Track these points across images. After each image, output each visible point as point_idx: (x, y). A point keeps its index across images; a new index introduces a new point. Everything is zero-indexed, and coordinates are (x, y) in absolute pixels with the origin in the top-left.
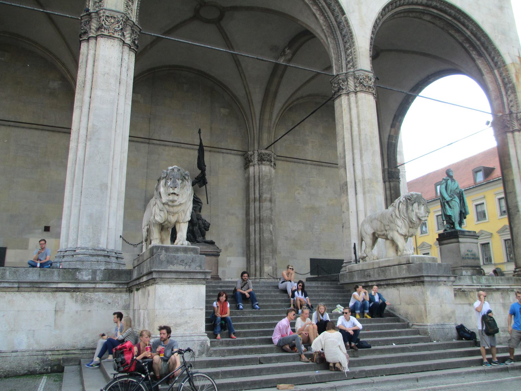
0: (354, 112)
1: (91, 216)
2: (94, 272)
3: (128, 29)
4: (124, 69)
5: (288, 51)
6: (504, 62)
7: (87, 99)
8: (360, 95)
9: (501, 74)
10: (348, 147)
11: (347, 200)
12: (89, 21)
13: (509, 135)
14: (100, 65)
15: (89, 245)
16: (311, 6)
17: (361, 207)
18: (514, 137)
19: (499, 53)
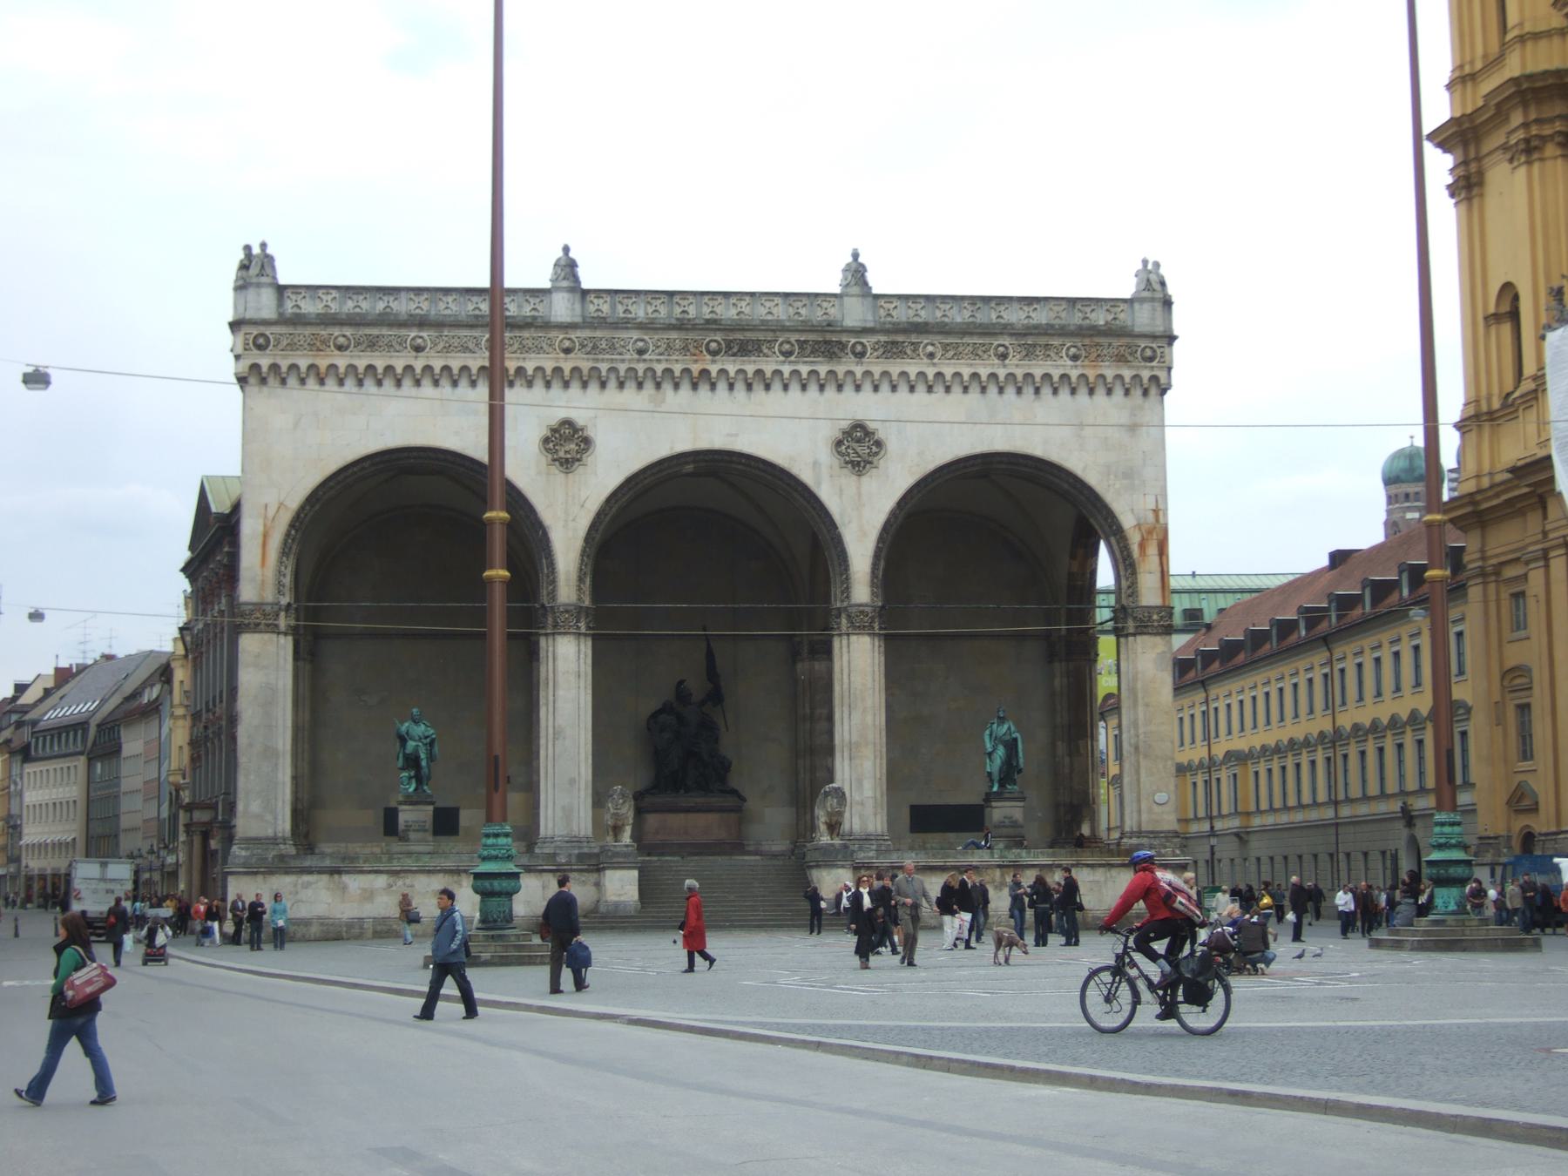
1: (563, 808)
8: (853, 638)
12: (545, 616)
14: (561, 666)
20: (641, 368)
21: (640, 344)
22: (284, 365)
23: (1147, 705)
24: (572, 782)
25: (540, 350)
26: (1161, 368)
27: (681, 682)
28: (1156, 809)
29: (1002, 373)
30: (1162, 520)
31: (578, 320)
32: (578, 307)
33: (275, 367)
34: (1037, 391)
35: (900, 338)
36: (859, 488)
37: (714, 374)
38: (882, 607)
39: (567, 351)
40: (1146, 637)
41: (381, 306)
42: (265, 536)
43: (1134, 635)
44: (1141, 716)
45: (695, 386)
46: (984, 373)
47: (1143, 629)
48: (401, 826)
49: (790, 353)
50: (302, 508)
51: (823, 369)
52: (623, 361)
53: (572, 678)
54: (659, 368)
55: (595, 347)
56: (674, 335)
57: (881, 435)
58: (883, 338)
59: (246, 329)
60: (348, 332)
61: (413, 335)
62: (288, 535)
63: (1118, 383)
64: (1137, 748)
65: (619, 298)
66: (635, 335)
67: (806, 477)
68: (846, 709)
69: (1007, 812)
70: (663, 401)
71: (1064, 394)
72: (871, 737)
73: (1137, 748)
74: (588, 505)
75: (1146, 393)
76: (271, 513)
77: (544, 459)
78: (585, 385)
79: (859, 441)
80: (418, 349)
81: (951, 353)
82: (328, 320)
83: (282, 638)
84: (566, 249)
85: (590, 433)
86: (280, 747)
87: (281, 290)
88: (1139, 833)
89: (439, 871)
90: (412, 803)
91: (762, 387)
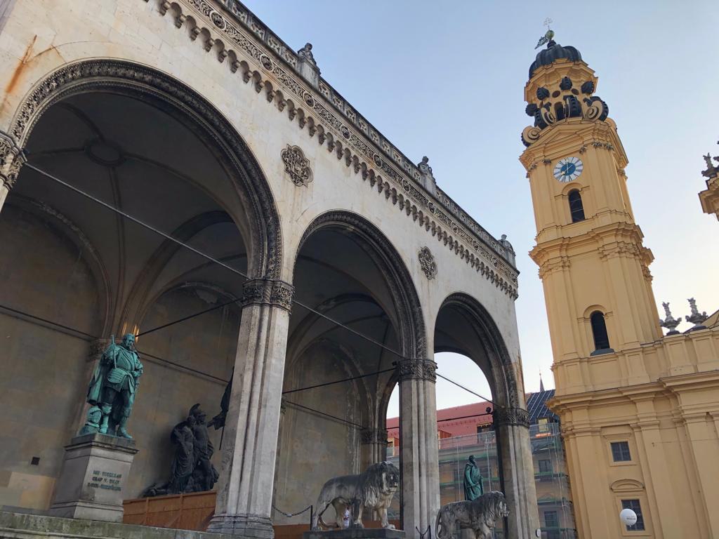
5: (332, 303)
6: (510, 361)
9: (506, 371)
10: (415, 429)
11: (412, 481)
13: (510, 427)
16: (392, 289)
17: (424, 489)
18: (513, 430)
19: (507, 352)
27: (198, 405)
40: (523, 427)
43: (517, 425)
48: (88, 479)
50: (72, 69)
52: (336, 133)
61: (215, 11)
64: (525, 496)
66: (344, 123)
70: (349, 176)
76: (40, 47)
77: (283, 166)
80: (218, 23)
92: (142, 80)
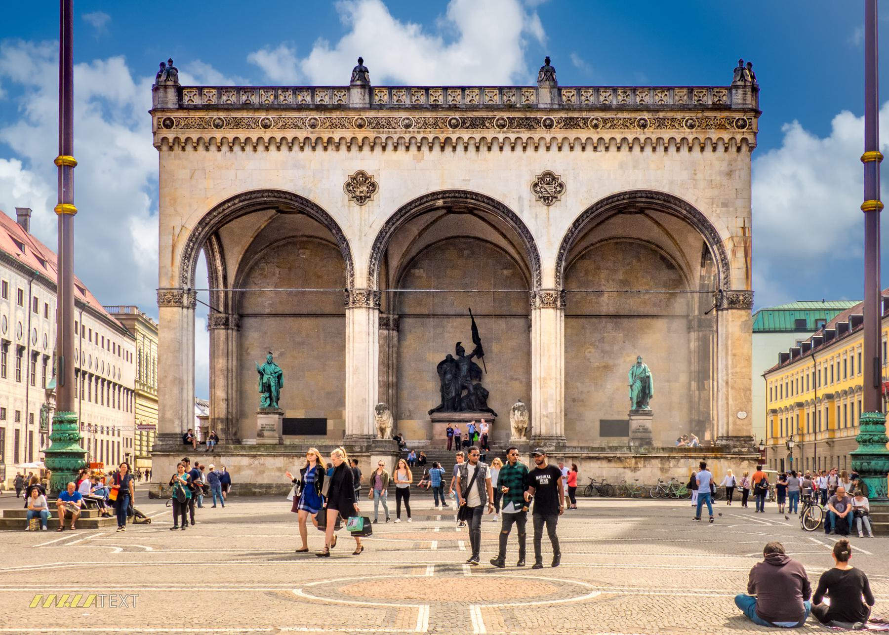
0: (538, 323)
1: (358, 417)
2: (361, 447)
3: (371, 298)
4: (371, 325)
7: (351, 348)
12: (348, 296)
14: (357, 328)
15: (359, 433)
20: (407, 137)
21: (407, 121)
22: (183, 138)
23: (734, 355)
24: (364, 400)
25: (343, 126)
26: (749, 133)
28: (738, 422)
29: (642, 138)
30: (747, 235)
31: (368, 106)
32: (367, 97)
33: (177, 139)
34: (666, 149)
35: (575, 115)
36: (548, 214)
37: (454, 141)
38: (563, 291)
39: (360, 126)
40: (734, 311)
41: (244, 98)
42: (174, 247)
43: (727, 309)
44: (730, 362)
45: (443, 149)
46: (630, 137)
47: (733, 304)
49: (504, 126)
50: (196, 228)
51: (525, 135)
52: (396, 133)
53: (364, 336)
54: (419, 137)
55: (378, 124)
56: (428, 115)
57: (562, 180)
58: (563, 115)
59: (159, 115)
60: (222, 115)
62: (188, 245)
63: (720, 144)
64: (727, 383)
65: (394, 92)
66: (403, 115)
67: (514, 207)
68: (538, 356)
69: (641, 423)
70: (422, 158)
71: (684, 150)
72: (553, 375)
73: (727, 383)
74: (373, 226)
75: (739, 149)
76: (177, 231)
77: (347, 197)
78: (372, 148)
79: (548, 184)
80: (266, 127)
81: (609, 125)
82: (208, 108)
83: (185, 310)
84: (361, 61)
85: (375, 179)
86: (185, 378)
87: (180, 90)
88: (728, 438)
89: (280, 456)
90: (266, 413)
91: (486, 148)
92: (234, 204)
